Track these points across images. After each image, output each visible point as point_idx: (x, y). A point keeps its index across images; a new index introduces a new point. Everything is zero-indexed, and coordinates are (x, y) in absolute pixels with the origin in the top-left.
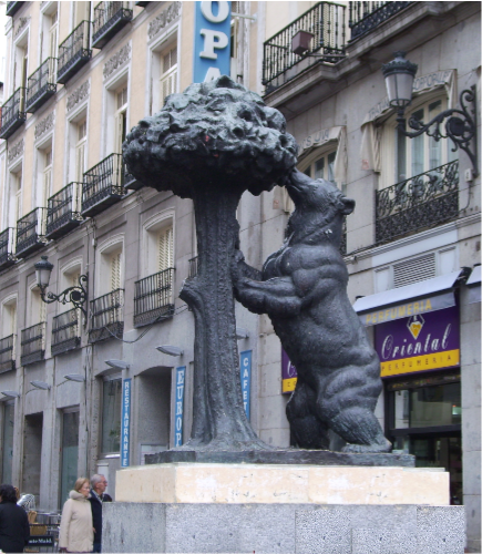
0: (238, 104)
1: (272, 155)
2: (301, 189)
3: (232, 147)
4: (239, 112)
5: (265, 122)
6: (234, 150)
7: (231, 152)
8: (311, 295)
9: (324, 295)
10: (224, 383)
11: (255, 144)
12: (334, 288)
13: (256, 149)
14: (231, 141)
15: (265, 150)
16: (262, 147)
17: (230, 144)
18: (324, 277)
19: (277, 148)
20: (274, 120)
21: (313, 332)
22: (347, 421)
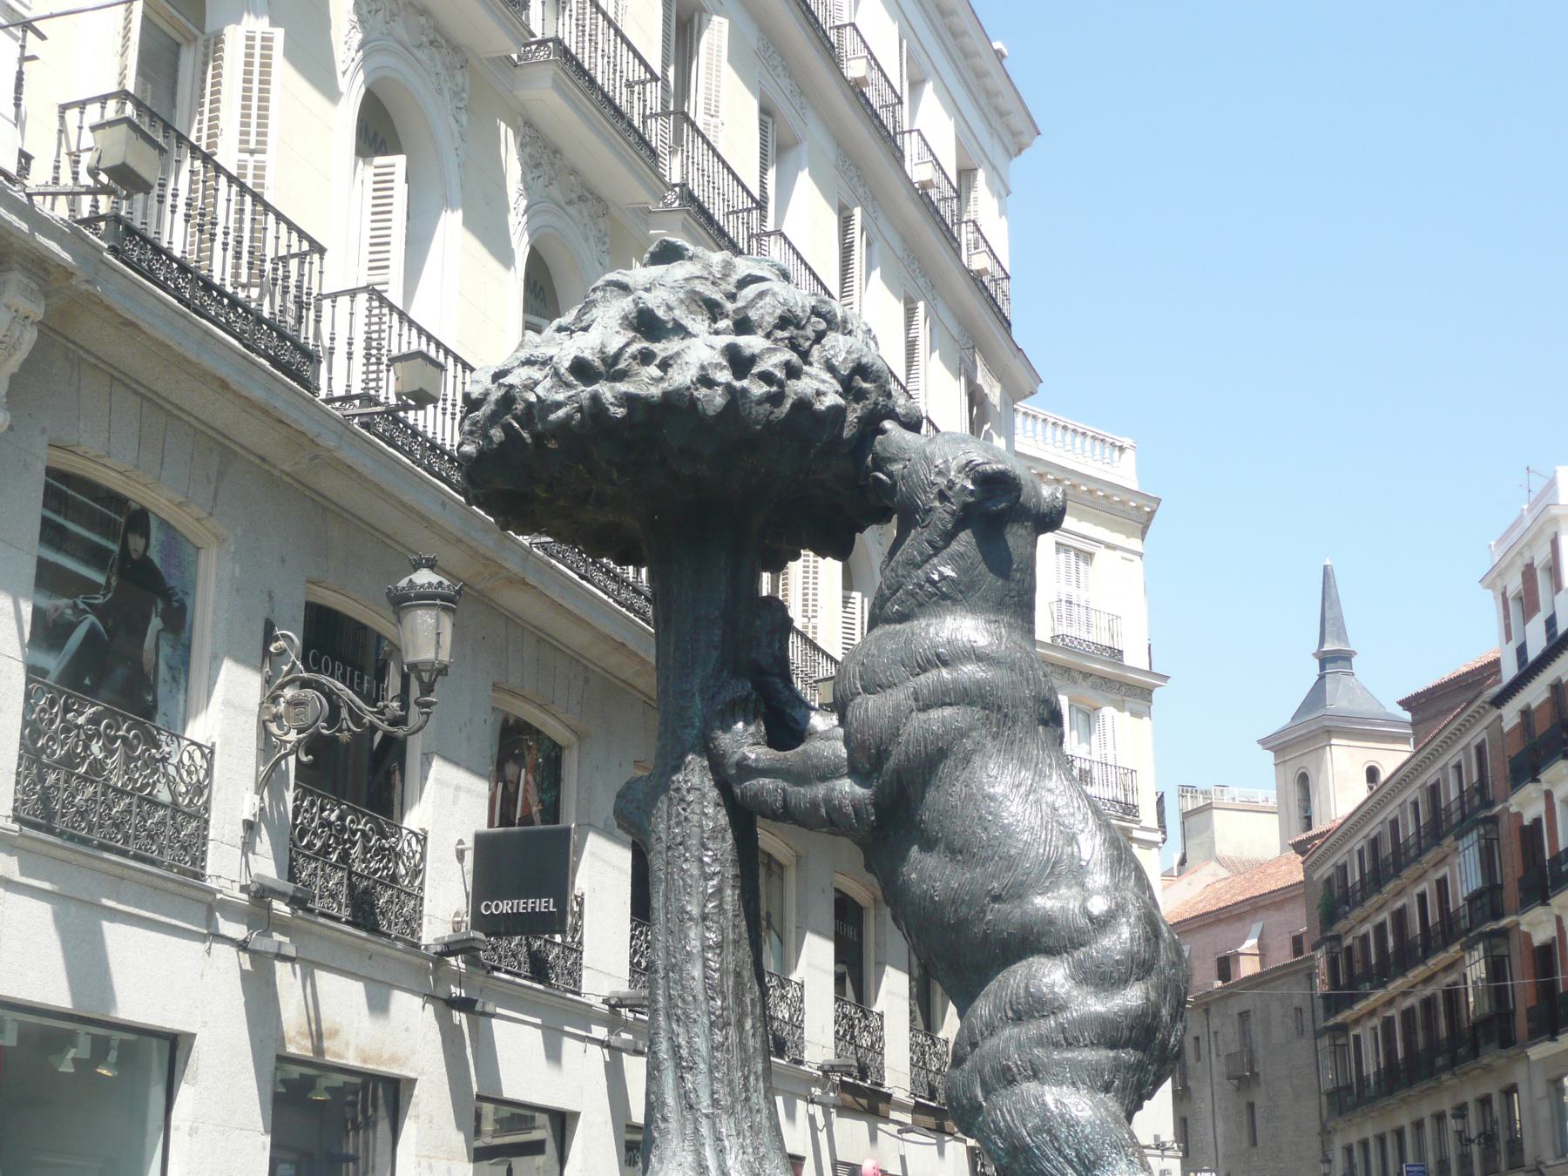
0: (625, 304)
1: (693, 401)
2: (890, 475)
3: (561, 413)
4: (625, 318)
5: (723, 324)
6: (569, 417)
7: (565, 422)
8: (891, 764)
9: (933, 760)
10: (675, 1049)
11: (623, 387)
12: (963, 734)
13: (628, 400)
14: (560, 396)
15: (666, 394)
16: (655, 391)
17: (558, 405)
18: (926, 708)
19: (706, 381)
20: (753, 315)
21: (927, 871)
22: (999, 1132)
